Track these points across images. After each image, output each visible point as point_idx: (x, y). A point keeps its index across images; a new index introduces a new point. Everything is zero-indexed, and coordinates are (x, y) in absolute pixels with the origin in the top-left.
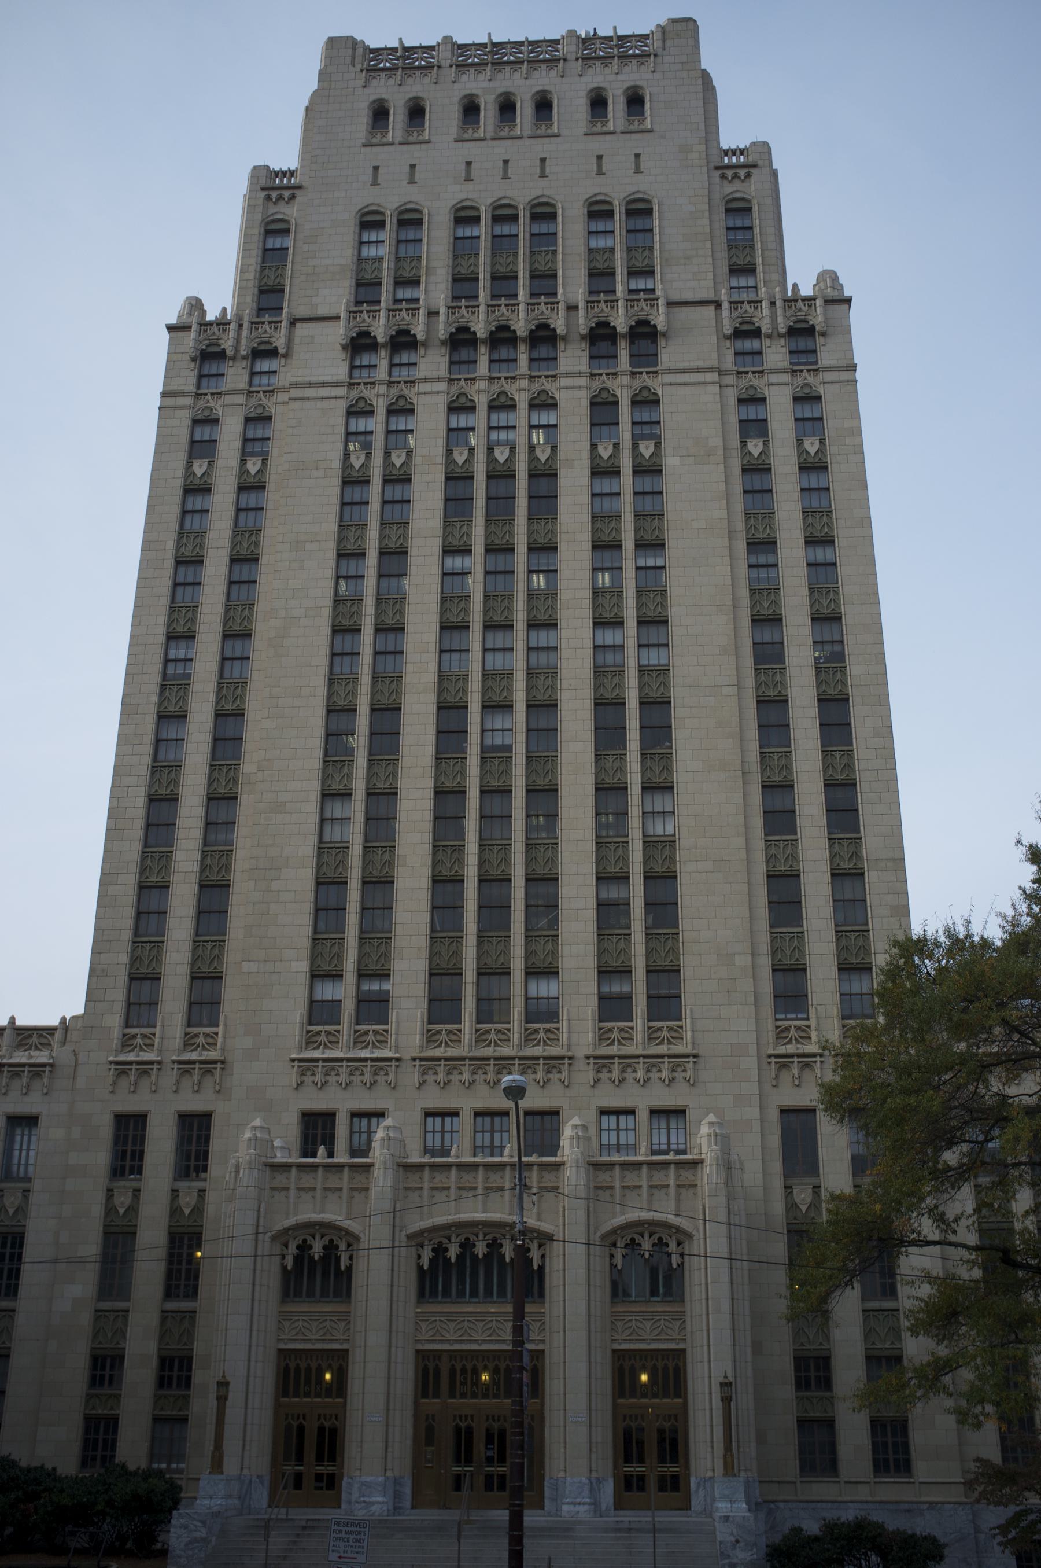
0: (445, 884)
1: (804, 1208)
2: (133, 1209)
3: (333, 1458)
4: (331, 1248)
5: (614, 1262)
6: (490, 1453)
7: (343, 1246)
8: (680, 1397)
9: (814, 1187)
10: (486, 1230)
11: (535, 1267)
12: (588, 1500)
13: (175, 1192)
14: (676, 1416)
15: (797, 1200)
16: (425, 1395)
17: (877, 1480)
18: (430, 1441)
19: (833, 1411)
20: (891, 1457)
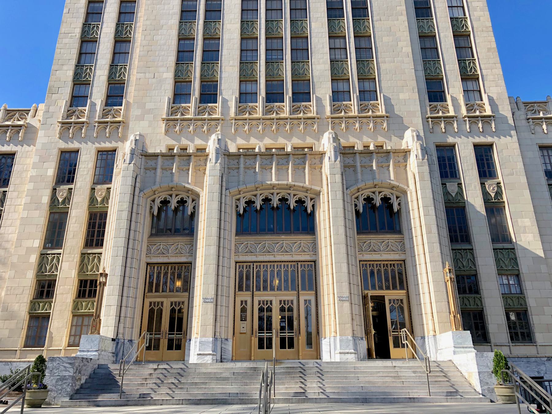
0: (247, 38)
1: (454, 195)
2: (67, 200)
3: (180, 329)
4: (182, 202)
5: (358, 208)
6: (283, 324)
7: (190, 201)
8: (403, 289)
9: (458, 184)
10: (278, 191)
11: (309, 211)
12: (353, 351)
13: (93, 189)
14: (402, 300)
15: (449, 190)
16: (241, 289)
17: (514, 344)
18: (243, 319)
19: (482, 305)
20: (519, 331)
